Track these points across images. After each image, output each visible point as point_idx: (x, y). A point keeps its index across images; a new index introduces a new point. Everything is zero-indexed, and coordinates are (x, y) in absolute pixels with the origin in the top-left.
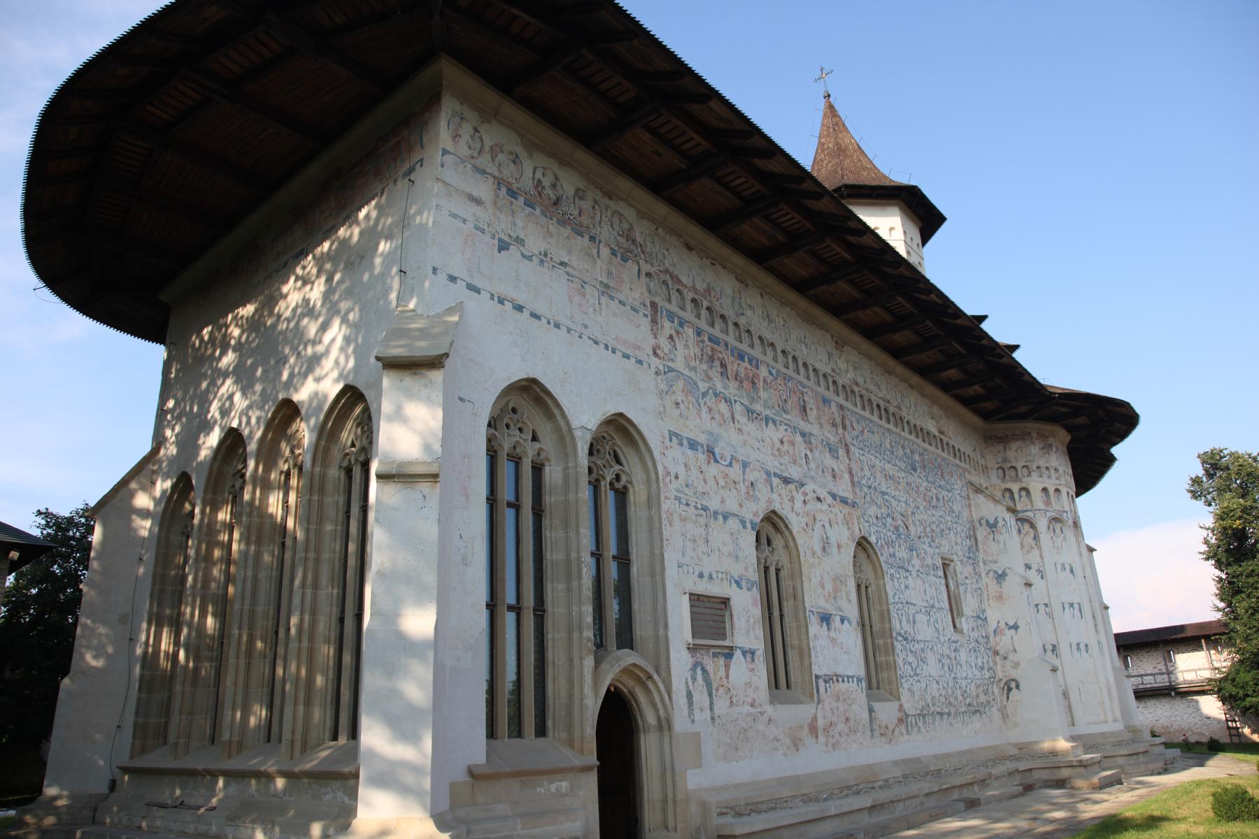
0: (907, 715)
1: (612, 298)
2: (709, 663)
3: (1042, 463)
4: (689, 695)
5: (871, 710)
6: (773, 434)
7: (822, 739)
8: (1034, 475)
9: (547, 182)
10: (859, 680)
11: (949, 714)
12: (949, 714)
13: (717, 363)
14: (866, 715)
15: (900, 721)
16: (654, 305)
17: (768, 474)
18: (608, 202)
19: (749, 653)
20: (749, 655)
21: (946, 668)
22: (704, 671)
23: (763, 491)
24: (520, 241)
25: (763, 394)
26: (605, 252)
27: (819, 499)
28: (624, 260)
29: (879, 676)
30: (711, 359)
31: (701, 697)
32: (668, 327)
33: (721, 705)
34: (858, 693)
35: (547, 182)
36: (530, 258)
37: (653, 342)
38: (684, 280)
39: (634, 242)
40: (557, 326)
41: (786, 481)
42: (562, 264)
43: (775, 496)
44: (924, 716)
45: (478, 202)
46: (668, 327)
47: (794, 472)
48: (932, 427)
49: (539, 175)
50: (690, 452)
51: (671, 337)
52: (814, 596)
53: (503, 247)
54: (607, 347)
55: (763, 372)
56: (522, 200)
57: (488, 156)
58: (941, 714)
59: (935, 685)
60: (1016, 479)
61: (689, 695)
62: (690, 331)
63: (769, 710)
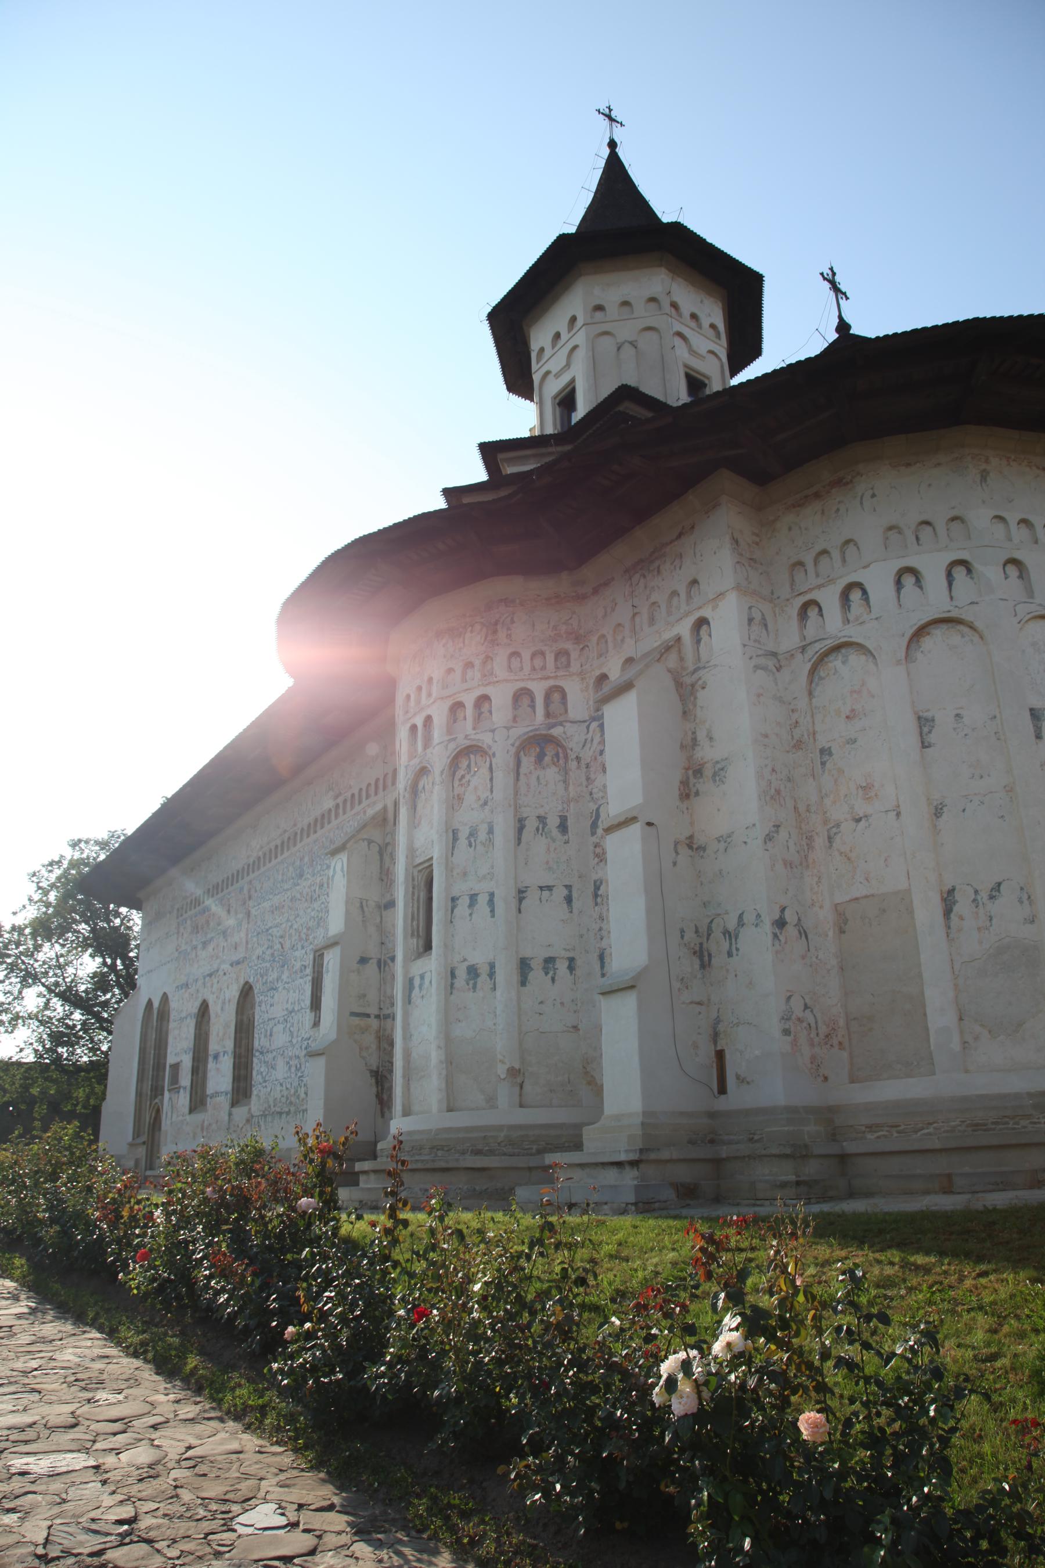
0: (252, 1116)
5: (230, 1114)
10: (226, 1094)
11: (288, 1113)
12: (288, 1113)
14: (227, 1118)
15: (248, 1121)
19: (185, 1088)
21: (293, 1069)
25: (212, 924)
29: (242, 1087)
31: (169, 1114)
34: (224, 1101)
44: (265, 1116)
47: (215, 966)
48: (329, 804)
52: (213, 1047)
58: (280, 1113)
59: (279, 1088)
63: (188, 1118)
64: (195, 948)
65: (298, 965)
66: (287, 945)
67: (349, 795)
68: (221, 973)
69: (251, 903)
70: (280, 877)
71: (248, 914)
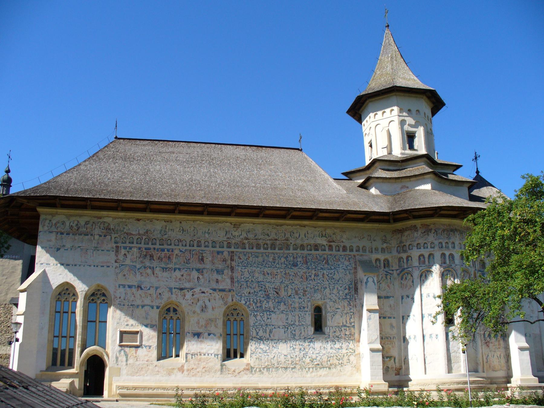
1: (98, 250)
2: (127, 349)
3: (421, 241)
4: (117, 358)
6: (178, 274)
7: (185, 372)
8: (415, 248)
9: (74, 225)
13: (148, 257)
16: (117, 247)
17: (171, 289)
18: (99, 220)
20: (148, 348)
22: (124, 351)
23: (166, 295)
24: (64, 246)
26: (97, 237)
27: (203, 292)
28: (105, 236)
30: (146, 256)
32: (123, 251)
33: (131, 361)
35: (74, 225)
36: (67, 250)
37: (116, 258)
38: (134, 233)
39: (109, 229)
40: (75, 265)
41: (181, 289)
42: (79, 247)
43: (174, 296)
45: (50, 241)
46: (123, 251)
47: (187, 285)
48: (323, 241)
49: (71, 224)
50: (128, 289)
51: (125, 254)
53: (58, 249)
54: (94, 266)
55: (176, 252)
56: (65, 234)
57: (54, 227)
60: (405, 251)
61: (117, 358)
62: (135, 250)
64: (153, 269)
65: (297, 305)
66: (283, 293)
67: (342, 244)
68: (197, 290)
69: (234, 263)
70: (271, 260)
71: (232, 269)
